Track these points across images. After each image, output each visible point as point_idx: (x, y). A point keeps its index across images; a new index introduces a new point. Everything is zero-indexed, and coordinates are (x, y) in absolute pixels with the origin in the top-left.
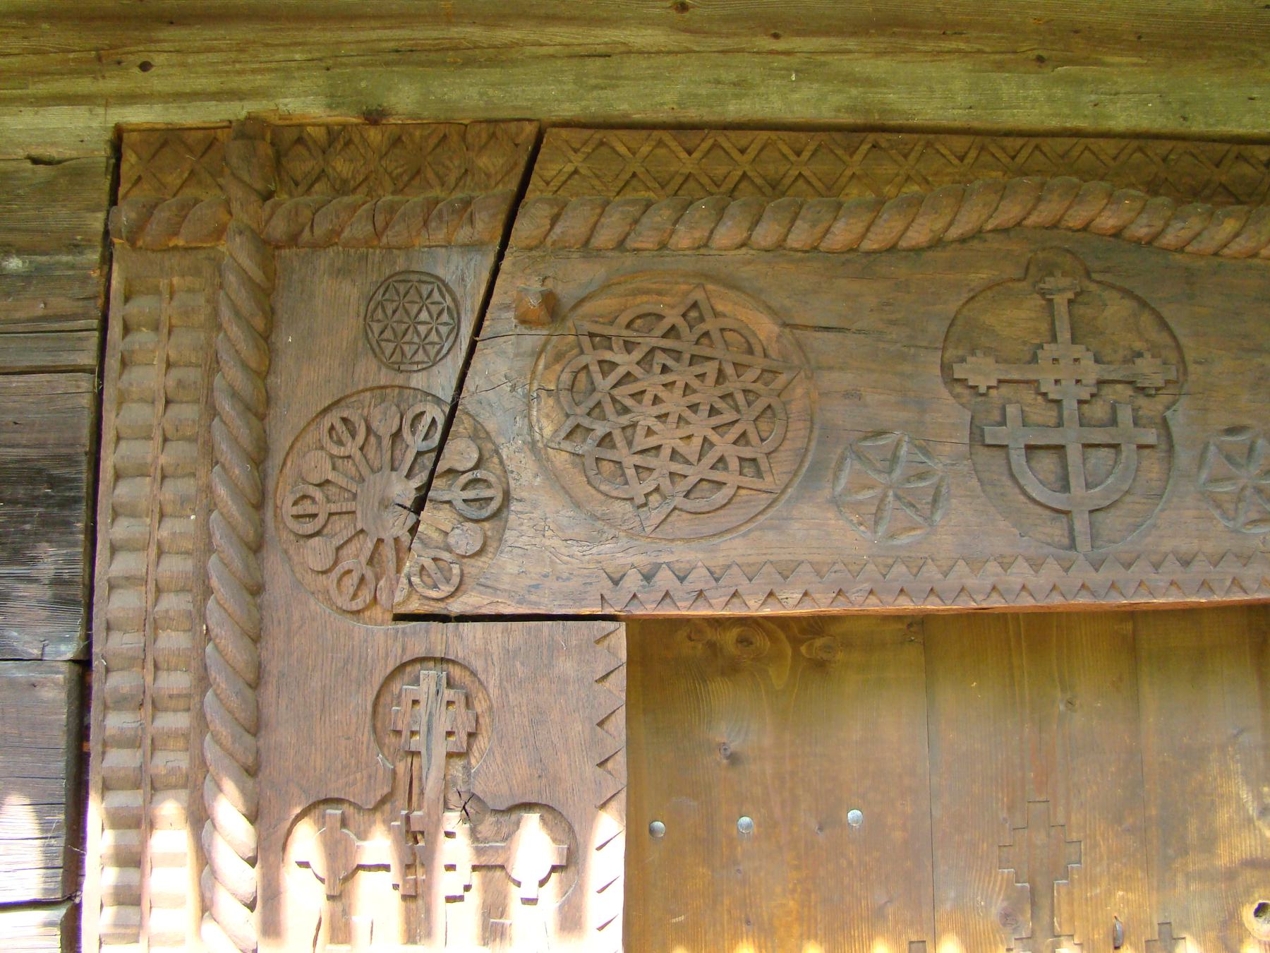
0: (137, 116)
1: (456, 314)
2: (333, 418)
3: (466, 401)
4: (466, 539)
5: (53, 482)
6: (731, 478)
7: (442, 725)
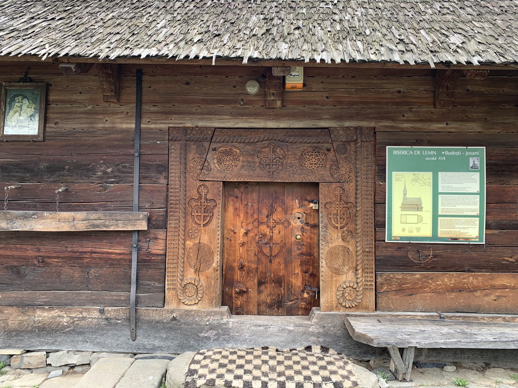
0: (171, 125)
1: (206, 149)
2: (193, 160)
3: (207, 159)
4: (206, 173)
5: (164, 166)
6: (234, 167)
7: (204, 191)
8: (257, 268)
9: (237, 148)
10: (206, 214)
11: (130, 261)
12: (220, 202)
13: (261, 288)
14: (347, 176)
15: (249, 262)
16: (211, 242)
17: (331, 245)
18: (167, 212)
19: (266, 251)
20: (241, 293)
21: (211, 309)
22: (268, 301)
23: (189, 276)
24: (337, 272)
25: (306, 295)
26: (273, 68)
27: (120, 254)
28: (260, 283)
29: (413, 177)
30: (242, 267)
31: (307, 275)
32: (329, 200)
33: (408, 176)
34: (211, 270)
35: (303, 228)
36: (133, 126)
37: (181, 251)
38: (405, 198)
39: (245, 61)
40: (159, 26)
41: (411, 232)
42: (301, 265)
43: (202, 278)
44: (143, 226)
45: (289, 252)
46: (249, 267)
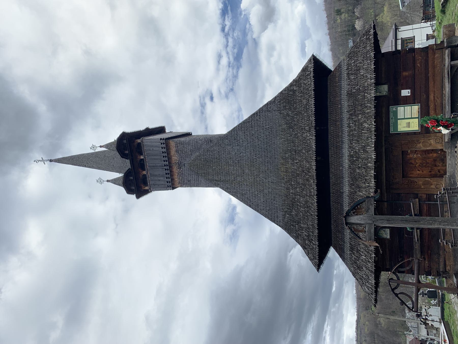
0: (385, 192)
8: (431, 167)
9: (392, 174)
10: (413, 182)
11: (429, 204)
12: (409, 179)
13: (438, 166)
14: (400, 143)
15: (429, 170)
16: (422, 181)
17: (422, 147)
18: (412, 194)
19: (425, 164)
20: (439, 171)
21: (444, 180)
22: (442, 163)
23: (433, 187)
24: (431, 144)
25: (439, 152)
27: (426, 207)
28: (436, 166)
29: (400, 125)
30: (430, 172)
31: (432, 152)
32: (407, 148)
33: (399, 127)
34: (431, 181)
35: (416, 154)
36: (386, 203)
37: (425, 189)
38: (406, 127)
39: (375, 173)
40: (362, 194)
41: (417, 125)
42: (429, 154)
43: (434, 183)
44: (417, 200)
45: (425, 158)
46: (430, 170)
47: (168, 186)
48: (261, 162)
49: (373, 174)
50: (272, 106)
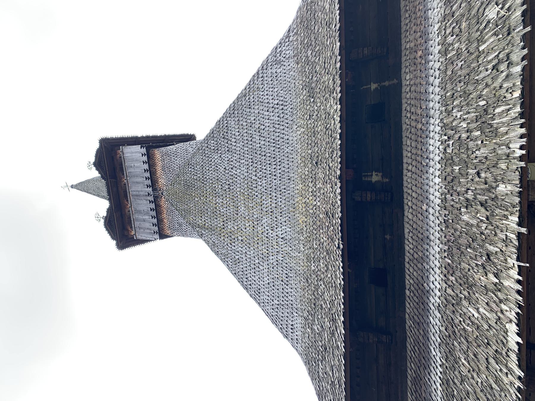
26: (530, 200)
39: (524, 230)
40: (476, 315)
47: (154, 232)
48: (265, 188)
49: (513, 232)
50: (284, 48)
